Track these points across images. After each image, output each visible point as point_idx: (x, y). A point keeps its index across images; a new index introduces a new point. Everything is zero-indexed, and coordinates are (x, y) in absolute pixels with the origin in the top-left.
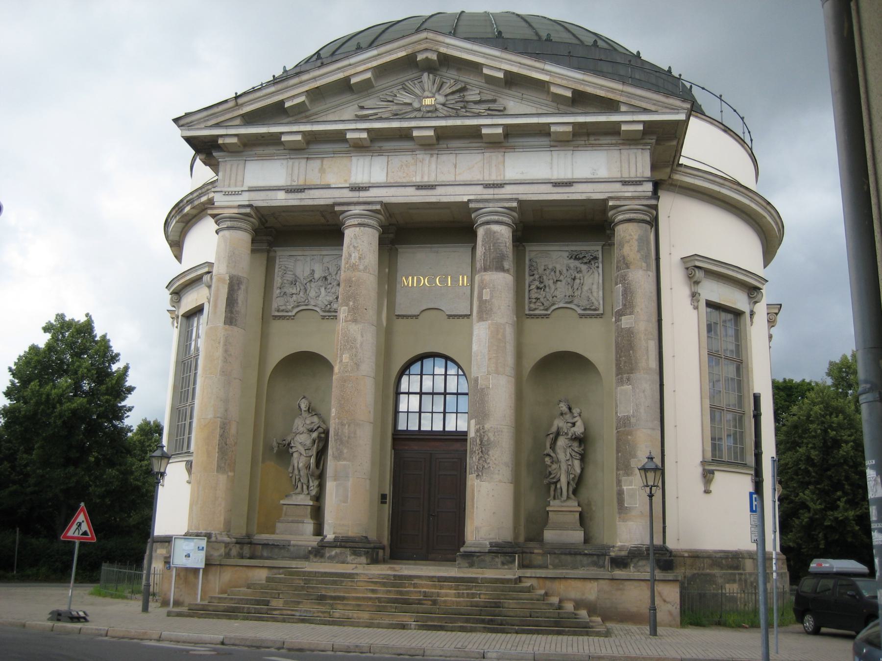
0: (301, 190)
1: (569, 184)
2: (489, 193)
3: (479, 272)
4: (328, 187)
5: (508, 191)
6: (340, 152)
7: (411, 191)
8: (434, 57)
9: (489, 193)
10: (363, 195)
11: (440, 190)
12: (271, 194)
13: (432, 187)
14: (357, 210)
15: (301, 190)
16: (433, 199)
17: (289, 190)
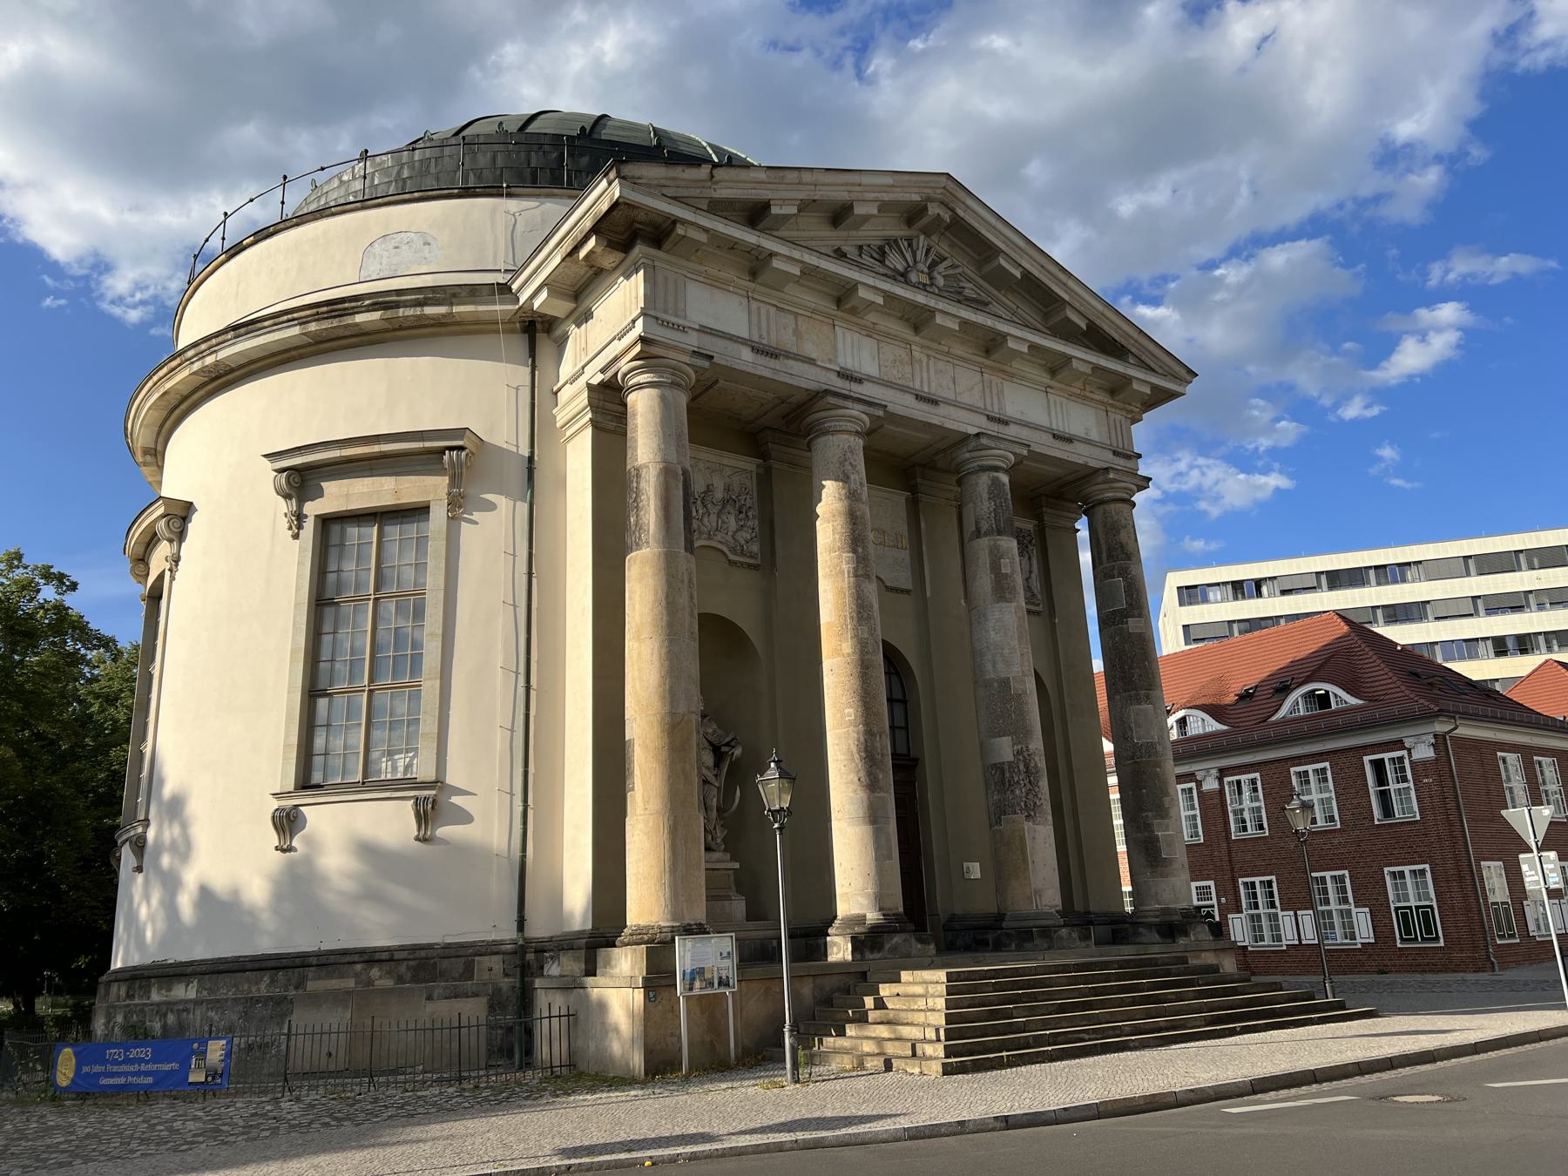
0: (773, 354)
1: (1069, 440)
2: (994, 428)
3: (986, 534)
4: (811, 362)
5: (1012, 431)
6: (821, 313)
7: (909, 400)
8: (947, 217)
9: (994, 428)
10: (857, 389)
11: (943, 410)
12: (732, 347)
13: (935, 402)
14: (856, 411)
15: (773, 354)
16: (935, 421)
17: (757, 350)
